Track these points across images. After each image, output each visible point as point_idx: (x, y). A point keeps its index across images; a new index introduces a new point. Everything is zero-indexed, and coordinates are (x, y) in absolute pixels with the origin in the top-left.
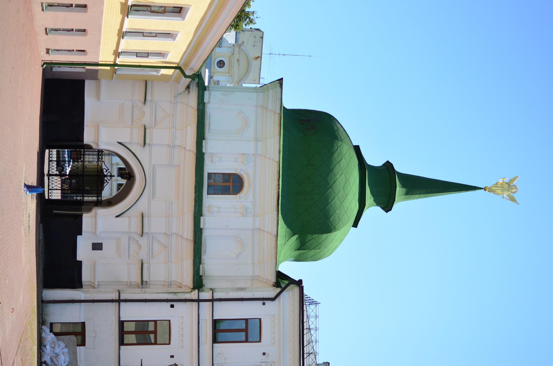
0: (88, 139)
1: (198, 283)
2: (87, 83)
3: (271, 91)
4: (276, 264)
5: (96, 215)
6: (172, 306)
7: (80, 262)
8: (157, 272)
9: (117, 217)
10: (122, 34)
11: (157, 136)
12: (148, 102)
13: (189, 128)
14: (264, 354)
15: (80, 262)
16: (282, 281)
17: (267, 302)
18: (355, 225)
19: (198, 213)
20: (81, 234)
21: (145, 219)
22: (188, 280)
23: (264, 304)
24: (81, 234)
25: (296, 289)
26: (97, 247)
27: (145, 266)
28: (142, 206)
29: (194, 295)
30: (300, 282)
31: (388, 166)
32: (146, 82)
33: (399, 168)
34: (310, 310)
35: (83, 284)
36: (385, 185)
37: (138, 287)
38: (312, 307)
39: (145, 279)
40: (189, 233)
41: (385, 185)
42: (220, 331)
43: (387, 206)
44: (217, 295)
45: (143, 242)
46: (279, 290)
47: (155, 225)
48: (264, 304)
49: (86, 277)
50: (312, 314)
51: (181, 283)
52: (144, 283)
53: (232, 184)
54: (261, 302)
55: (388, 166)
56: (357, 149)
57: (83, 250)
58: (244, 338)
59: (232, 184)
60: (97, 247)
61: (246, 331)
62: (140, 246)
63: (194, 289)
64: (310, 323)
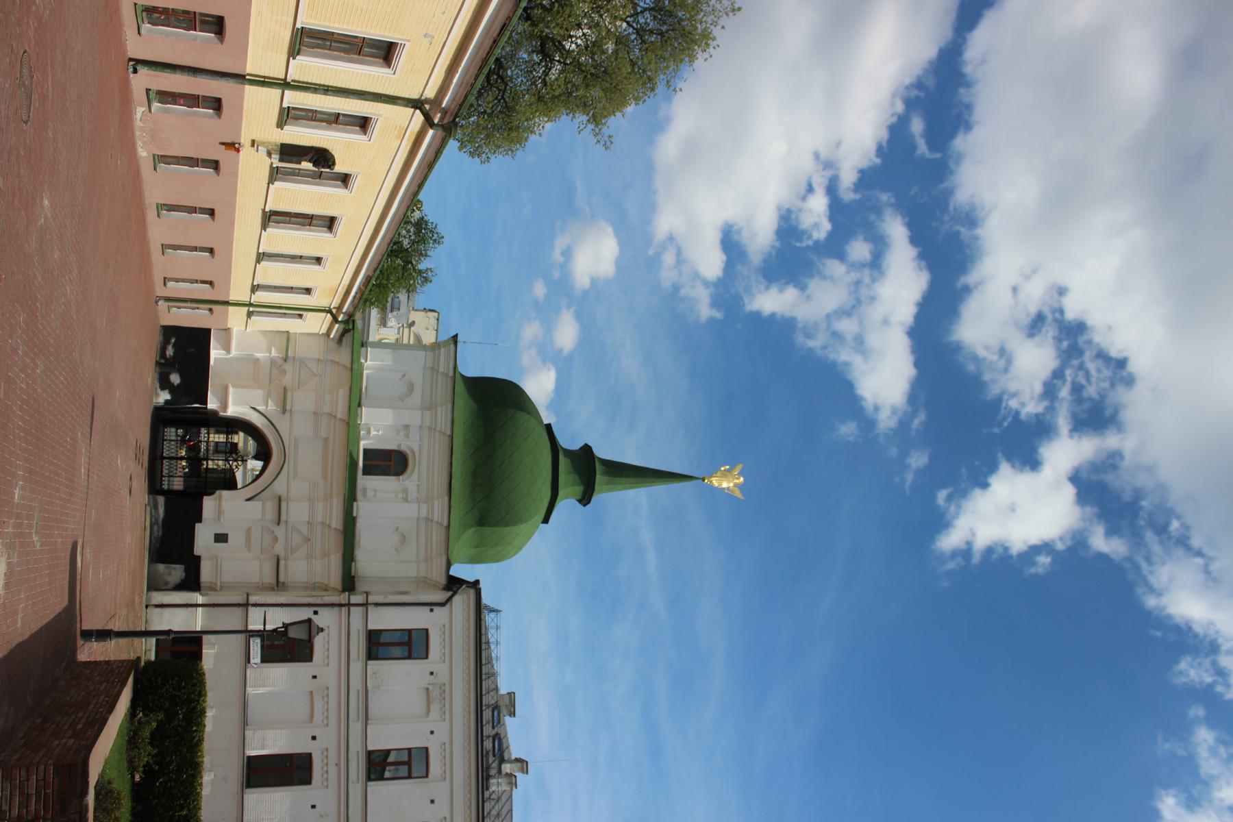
1: (349, 583)
4: (449, 565)
5: (220, 498)
7: (199, 557)
8: (297, 570)
10: (261, 257)
14: (432, 673)
15: (199, 557)
16: (454, 584)
17: (436, 609)
19: (351, 497)
20: (200, 521)
21: (284, 504)
22: (336, 580)
24: (200, 521)
25: (472, 592)
26: (221, 538)
27: (282, 563)
28: (280, 487)
29: (343, 598)
30: (477, 582)
31: (587, 449)
33: (601, 452)
34: (489, 619)
37: (272, 589)
38: (493, 615)
39: (282, 579)
40: (337, 522)
42: (378, 645)
43: (585, 499)
44: (372, 599)
45: (280, 532)
46: (450, 593)
47: (297, 512)
50: (492, 624)
54: (428, 608)
55: (587, 449)
57: (203, 536)
58: (406, 654)
60: (221, 538)
61: (411, 645)
62: (276, 539)
63: (344, 591)
64: (492, 635)
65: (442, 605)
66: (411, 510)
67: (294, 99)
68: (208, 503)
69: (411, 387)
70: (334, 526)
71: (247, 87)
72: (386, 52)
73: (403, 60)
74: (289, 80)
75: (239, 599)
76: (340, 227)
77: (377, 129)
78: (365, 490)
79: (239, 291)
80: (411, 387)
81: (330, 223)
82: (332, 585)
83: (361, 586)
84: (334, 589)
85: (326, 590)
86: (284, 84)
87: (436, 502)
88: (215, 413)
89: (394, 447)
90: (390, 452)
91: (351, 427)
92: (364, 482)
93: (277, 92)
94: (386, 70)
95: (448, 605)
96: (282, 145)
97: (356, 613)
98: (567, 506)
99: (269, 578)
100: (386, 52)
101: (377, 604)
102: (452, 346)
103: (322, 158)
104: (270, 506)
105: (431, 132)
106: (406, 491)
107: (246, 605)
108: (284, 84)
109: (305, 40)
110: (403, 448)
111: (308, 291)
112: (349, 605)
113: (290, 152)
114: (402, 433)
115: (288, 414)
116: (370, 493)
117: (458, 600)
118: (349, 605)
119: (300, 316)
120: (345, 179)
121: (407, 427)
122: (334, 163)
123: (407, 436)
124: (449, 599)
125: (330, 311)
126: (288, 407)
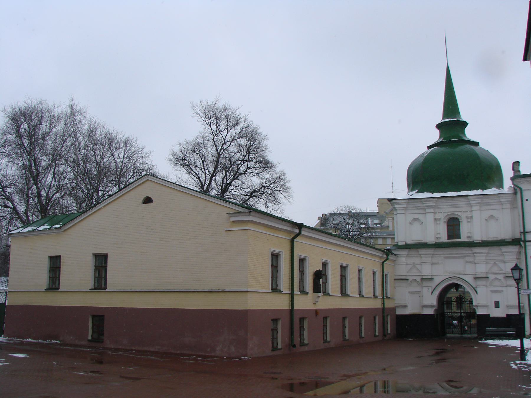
0: (430, 312)
1: (515, 242)
3: (396, 206)
5: (477, 306)
7: (507, 315)
9: (477, 293)
10: (361, 295)
11: (427, 270)
12: (407, 278)
13: (420, 253)
18: (477, 144)
19: (471, 244)
20: (489, 315)
21: (478, 276)
23: (527, 200)
24: (489, 315)
26: (497, 305)
31: (439, 126)
32: (395, 279)
36: (452, 126)
41: (452, 126)
43: (465, 124)
45: (491, 277)
47: (481, 269)
49: (516, 312)
53: (453, 225)
59: (453, 225)
60: (497, 305)
66: (476, 215)
67: (296, 291)
69: (416, 219)
70: (487, 251)
71: (295, 308)
72: (275, 257)
73: (277, 250)
74: (289, 292)
76: (345, 263)
77: (303, 255)
78: (468, 237)
79: (377, 304)
80: (416, 219)
81: (343, 268)
83: (518, 236)
86: (292, 294)
87: (471, 202)
88: (436, 310)
89: (446, 224)
90: (448, 226)
91: (438, 246)
92: (464, 237)
93: (295, 297)
94: (282, 255)
96: (314, 292)
98: (470, 134)
100: (275, 257)
102: (393, 201)
103: (318, 275)
104: (480, 283)
105: (303, 232)
106: (467, 217)
108: (292, 294)
109: (275, 289)
111: (374, 273)
113: (317, 288)
114: (438, 222)
115: (433, 277)
116: (469, 235)
119: (386, 275)
120: (325, 265)
121: (435, 220)
122: (319, 270)
123: (439, 219)
125: (383, 263)
126: (430, 277)
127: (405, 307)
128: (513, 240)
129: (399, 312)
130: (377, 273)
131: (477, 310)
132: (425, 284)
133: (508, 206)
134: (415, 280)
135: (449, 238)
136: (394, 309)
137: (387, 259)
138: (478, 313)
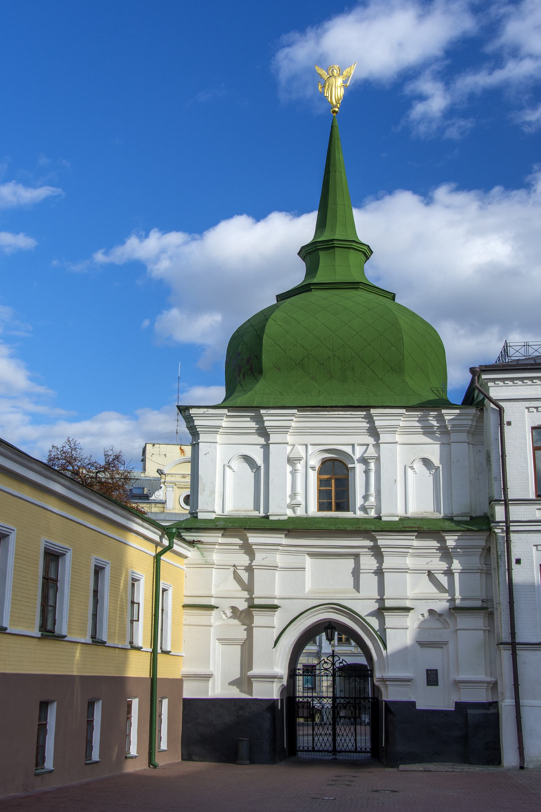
2: (187, 694)
6: (518, 561)
7: (457, 704)
10: (97, 642)
15: (457, 703)
20: (414, 703)
23: (509, 423)
24: (414, 703)
26: (432, 677)
30: (472, 371)
35: (491, 700)
38: (511, 351)
39: (478, 604)
48: (509, 423)
49: (481, 696)
50: (522, 351)
51: (483, 549)
52: (485, 605)
54: (506, 427)
56: (281, 298)
60: (432, 677)
65: (501, 411)
68: (391, 694)
75: (506, 655)
81: (53, 557)
82: (483, 543)
84: (488, 540)
85: (489, 550)
95: (501, 404)
97: (518, 513)
98: (371, 272)
99: (478, 621)
101: (505, 489)
102: (192, 411)
107: (513, 646)
110: (315, 462)
112: (507, 521)
117: (496, 392)
118: (507, 521)
124: (495, 402)
127: (207, 677)
128: (472, 518)
129: (190, 691)
130: (142, 583)
131: (383, 689)
132: (259, 618)
133: (464, 436)
134: (234, 609)
135: (321, 507)
136: (177, 684)
137: (169, 548)
138: (384, 698)
